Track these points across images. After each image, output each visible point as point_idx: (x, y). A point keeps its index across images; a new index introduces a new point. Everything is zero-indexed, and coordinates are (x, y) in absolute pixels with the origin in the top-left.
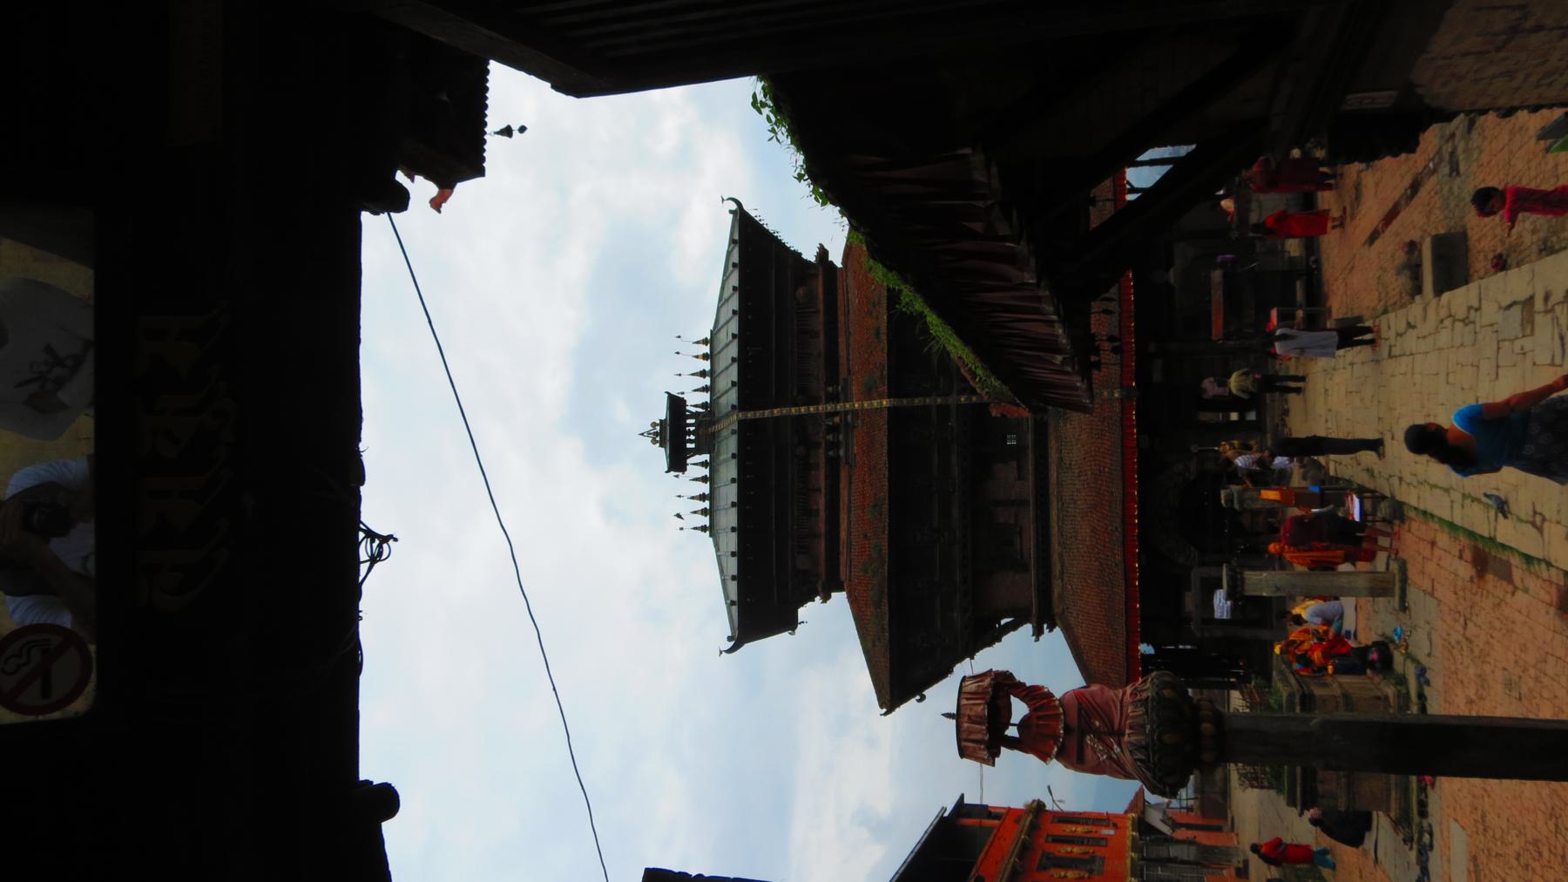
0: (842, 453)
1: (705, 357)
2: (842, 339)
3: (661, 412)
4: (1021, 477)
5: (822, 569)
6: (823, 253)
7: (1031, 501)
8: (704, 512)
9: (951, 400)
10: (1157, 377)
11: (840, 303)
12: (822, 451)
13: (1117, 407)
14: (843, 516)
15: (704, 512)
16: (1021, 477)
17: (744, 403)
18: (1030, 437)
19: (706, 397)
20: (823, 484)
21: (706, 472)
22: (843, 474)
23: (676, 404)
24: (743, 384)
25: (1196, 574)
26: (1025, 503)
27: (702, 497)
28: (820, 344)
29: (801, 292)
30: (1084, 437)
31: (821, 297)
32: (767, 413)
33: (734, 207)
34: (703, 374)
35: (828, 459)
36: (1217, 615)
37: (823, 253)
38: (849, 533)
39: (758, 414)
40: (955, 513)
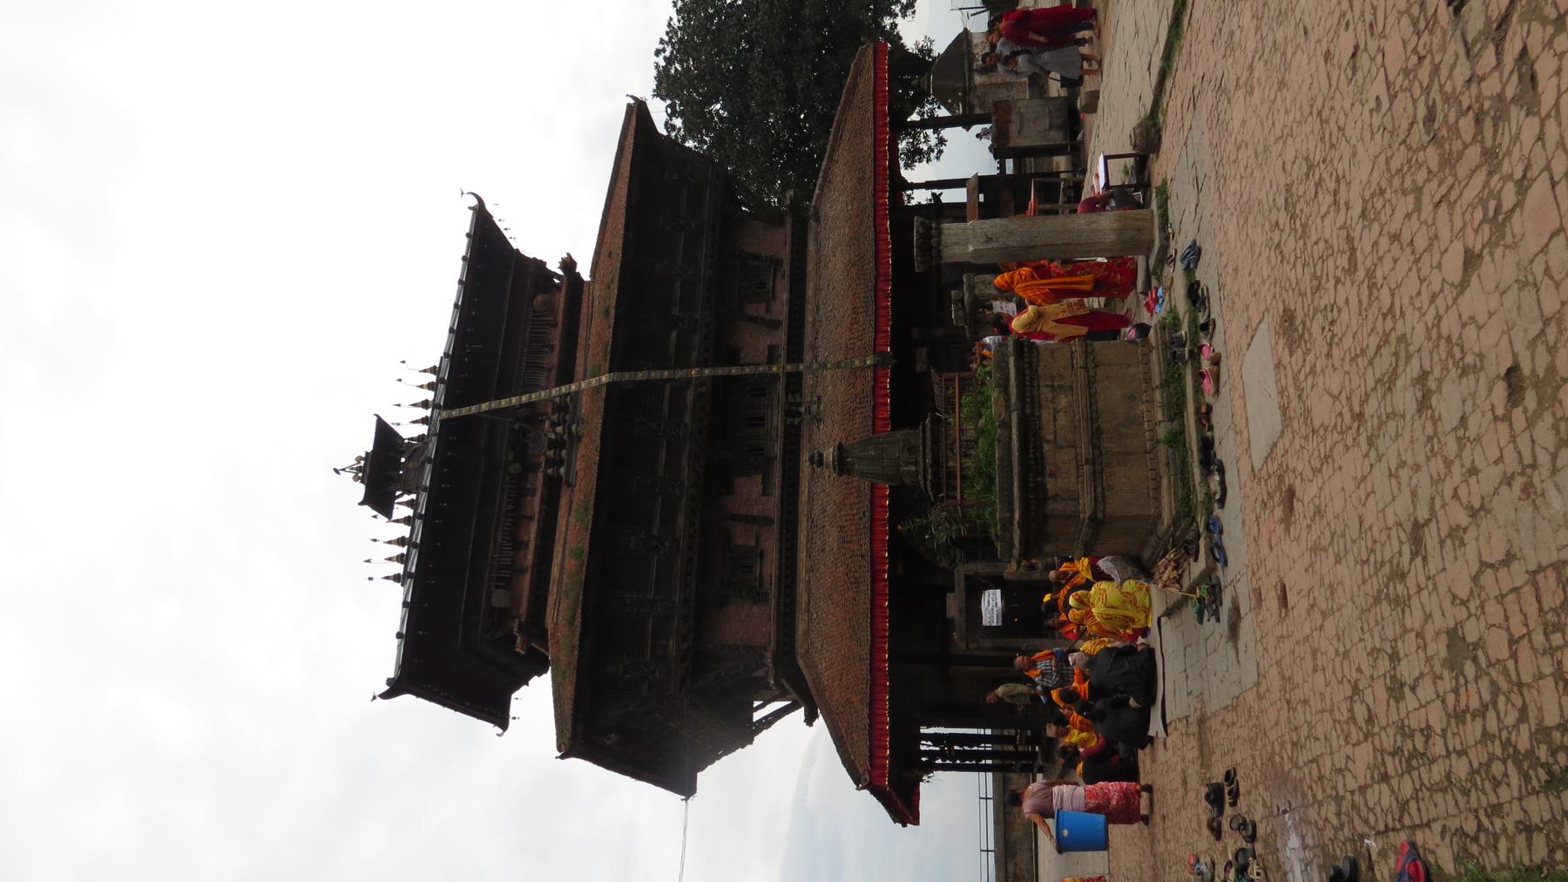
0: (562, 470)
1: (431, 386)
2: (580, 354)
3: (367, 444)
4: (765, 493)
5: (523, 609)
6: (569, 264)
8: (401, 559)
9: (680, 374)
11: (583, 318)
13: (870, 374)
14: (558, 549)
15: (401, 559)
16: (765, 492)
18: (778, 448)
20: (537, 508)
21: (409, 512)
22: (564, 501)
23: (384, 433)
25: (963, 570)
26: (766, 521)
28: (553, 359)
29: (539, 298)
34: (425, 404)
35: (547, 477)
36: (986, 622)
38: (562, 567)
40: (681, 520)
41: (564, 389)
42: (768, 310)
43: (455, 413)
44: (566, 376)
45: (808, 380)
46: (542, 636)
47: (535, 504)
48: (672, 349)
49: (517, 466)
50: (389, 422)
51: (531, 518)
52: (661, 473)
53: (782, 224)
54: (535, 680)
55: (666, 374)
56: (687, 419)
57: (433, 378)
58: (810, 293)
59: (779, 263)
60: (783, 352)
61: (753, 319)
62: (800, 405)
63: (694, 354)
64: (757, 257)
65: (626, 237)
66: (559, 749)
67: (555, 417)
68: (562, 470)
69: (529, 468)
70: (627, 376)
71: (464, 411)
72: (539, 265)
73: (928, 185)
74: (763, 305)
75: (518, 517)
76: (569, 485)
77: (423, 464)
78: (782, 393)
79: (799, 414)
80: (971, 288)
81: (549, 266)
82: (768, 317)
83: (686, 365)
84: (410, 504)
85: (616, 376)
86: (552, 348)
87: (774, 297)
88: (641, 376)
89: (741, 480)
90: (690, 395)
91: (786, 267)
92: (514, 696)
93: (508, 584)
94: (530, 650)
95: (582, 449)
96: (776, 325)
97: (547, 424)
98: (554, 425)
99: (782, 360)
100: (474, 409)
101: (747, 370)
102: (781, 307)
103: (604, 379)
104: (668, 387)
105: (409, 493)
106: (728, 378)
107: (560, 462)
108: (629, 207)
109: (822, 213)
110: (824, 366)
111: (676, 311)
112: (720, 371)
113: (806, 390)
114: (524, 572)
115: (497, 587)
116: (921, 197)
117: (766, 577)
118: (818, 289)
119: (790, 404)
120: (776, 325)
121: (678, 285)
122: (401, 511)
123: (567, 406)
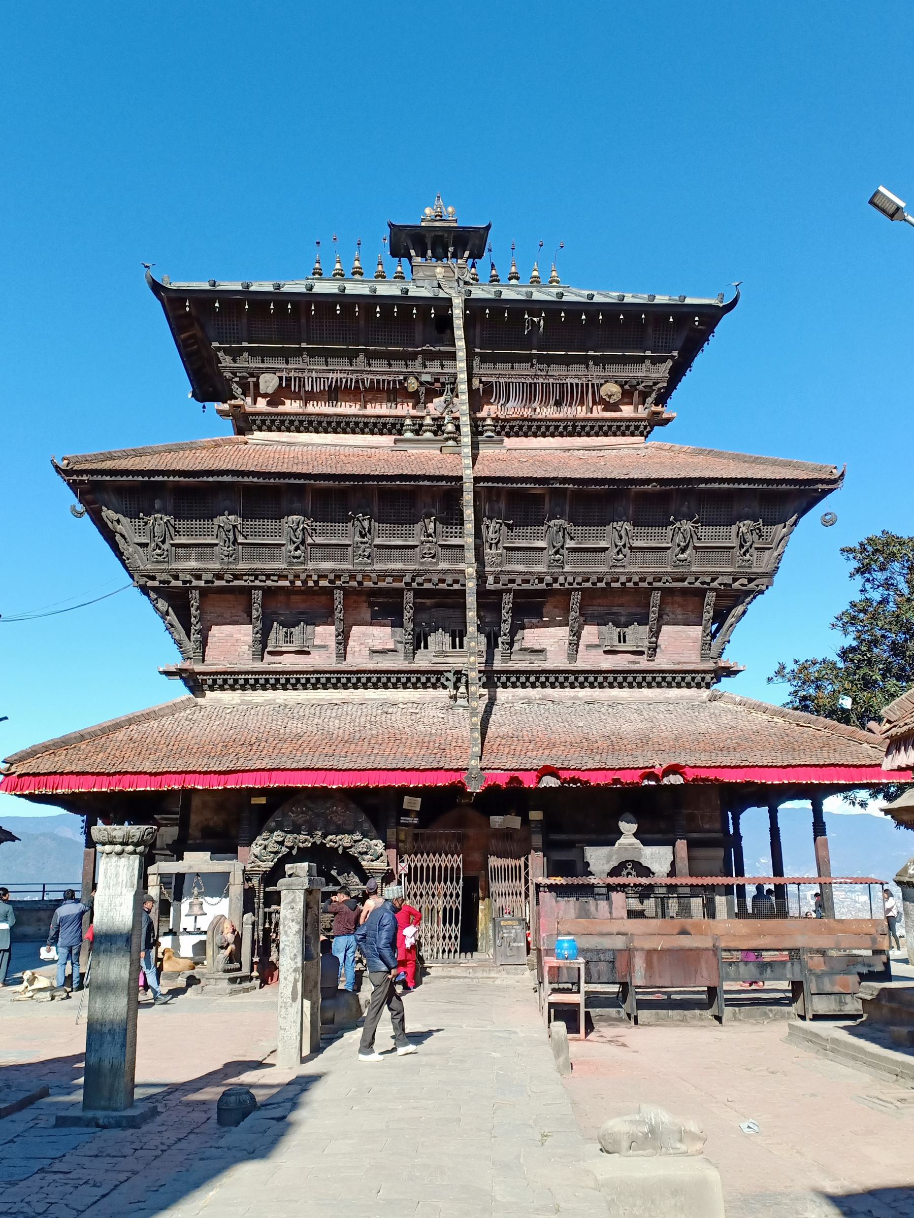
0: (409, 435)
7: (343, 666)
10: (497, 821)
12: (414, 412)
24: (497, 305)
28: (549, 412)
30: (421, 727)
32: (459, 333)
39: (458, 322)
50: (491, 239)
53: (703, 657)
63: (521, 568)
68: (409, 435)
70: (468, 497)
82: (581, 647)
85: (468, 486)
87: (606, 652)
96: (572, 657)
100: (459, 333)
102: (589, 660)
103: (468, 474)
106: (463, 607)
107: (417, 432)
115: (281, 378)
120: (572, 657)
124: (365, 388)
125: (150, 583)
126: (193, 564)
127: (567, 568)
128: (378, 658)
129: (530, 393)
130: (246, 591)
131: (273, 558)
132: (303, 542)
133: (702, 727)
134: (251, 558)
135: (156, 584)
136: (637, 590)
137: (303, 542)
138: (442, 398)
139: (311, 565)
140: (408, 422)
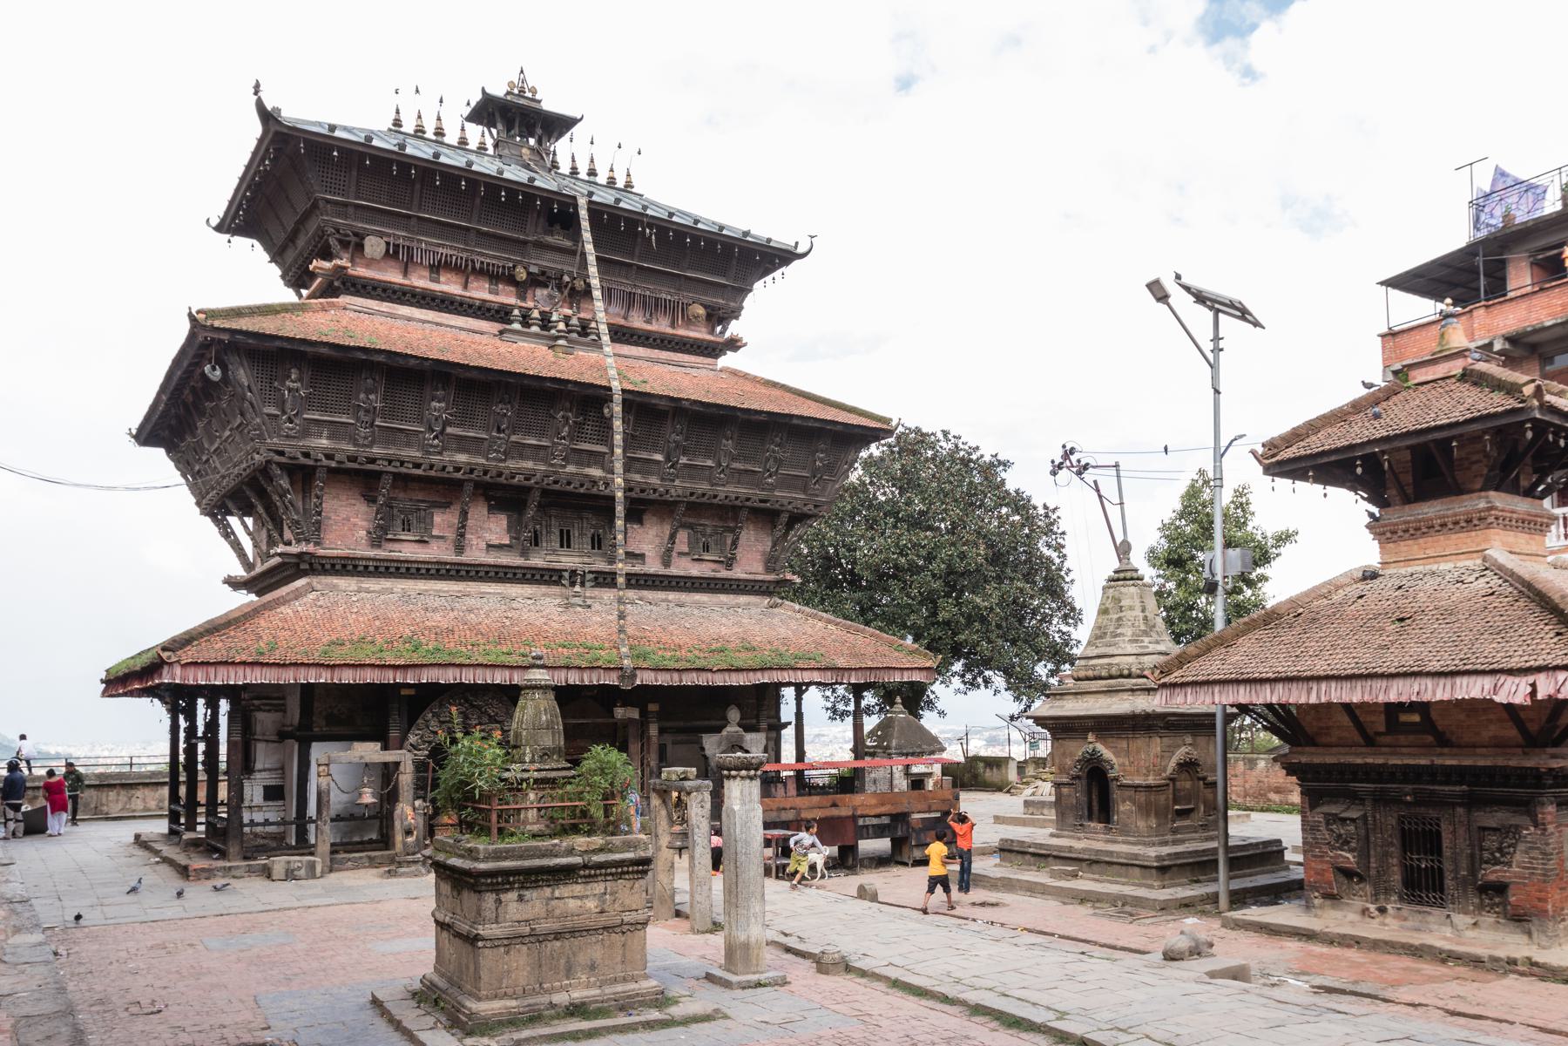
1: (611, 182)
4: (489, 546)
5: (361, 271)
7: (463, 559)
8: (419, 132)
15: (419, 132)
17: (596, 210)
18: (537, 561)
19: (565, 169)
21: (473, 145)
27: (439, 132)
28: (637, 321)
29: (701, 311)
31: (692, 334)
33: (800, 250)
34: (592, 173)
37: (734, 344)
38: (409, 319)
40: (462, 458)
41: (603, 328)
42: (681, 554)
43: (583, 213)
44: (621, 335)
45: (608, 595)
46: (329, 291)
47: (480, 291)
48: (644, 455)
49: (524, 276)
50: (575, 130)
51: (465, 287)
52: (514, 438)
53: (768, 570)
54: (275, 271)
55: (618, 451)
56: (571, 469)
57: (620, 184)
58: (698, 597)
59: (729, 563)
60: (638, 569)
61: (672, 537)
62: (583, 584)
63: (638, 477)
64: (735, 544)
65: (762, 412)
66: (198, 312)
67: (574, 321)
69: (522, 288)
70: (618, 409)
71: (585, 224)
72: (735, 314)
73: (799, 715)
74: (686, 549)
75: (467, 271)
76: (501, 332)
77: (527, 167)
78: (595, 567)
79: (573, 584)
80: (698, 789)
81: (734, 322)
83: (627, 469)
84: (482, 148)
85: (618, 398)
86: (648, 322)
88: (618, 424)
89: (505, 522)
90: (596, 472)
91: (724, 574)
92: (255, 242)
93: (392, 254)
94: (313, 276)
95: (542, 350)
96: (667, 564)
97: (569, 312)
98: (567, 319)
99: (629, 568)
100: (587, 235)
101: (620, 537)
103: (616, 385)
104: (603, 449)
105: (496, 146)
108: (791, 416)
109: (776, 610)
110: (622, 616)
111: (684, 460)
112: (620, 509)
113: (597, 592)
114: (405, 273)
115: (388, 244)
116: (787, 712)
117: (396, 546)
118: (699, 606)
119: (583, 576)
120: (667, 564)
121: (709, 463)
122: (475, 133)
123: (587, 335)
124: (474, 268)
125: (277, 458)
126: (324, 442)
127: (677, 483)
128: (493, 553)
129: (630, 301)
130: (378, 475)
131: (409, 445)
132: (442, 432)
133: (783, 632)
134: (387, 443)
135: (283, 460)
136: (734, 507)
137: (442, 432)
138: (545, 292)
139: (446, 457)
140: (516, 312)
